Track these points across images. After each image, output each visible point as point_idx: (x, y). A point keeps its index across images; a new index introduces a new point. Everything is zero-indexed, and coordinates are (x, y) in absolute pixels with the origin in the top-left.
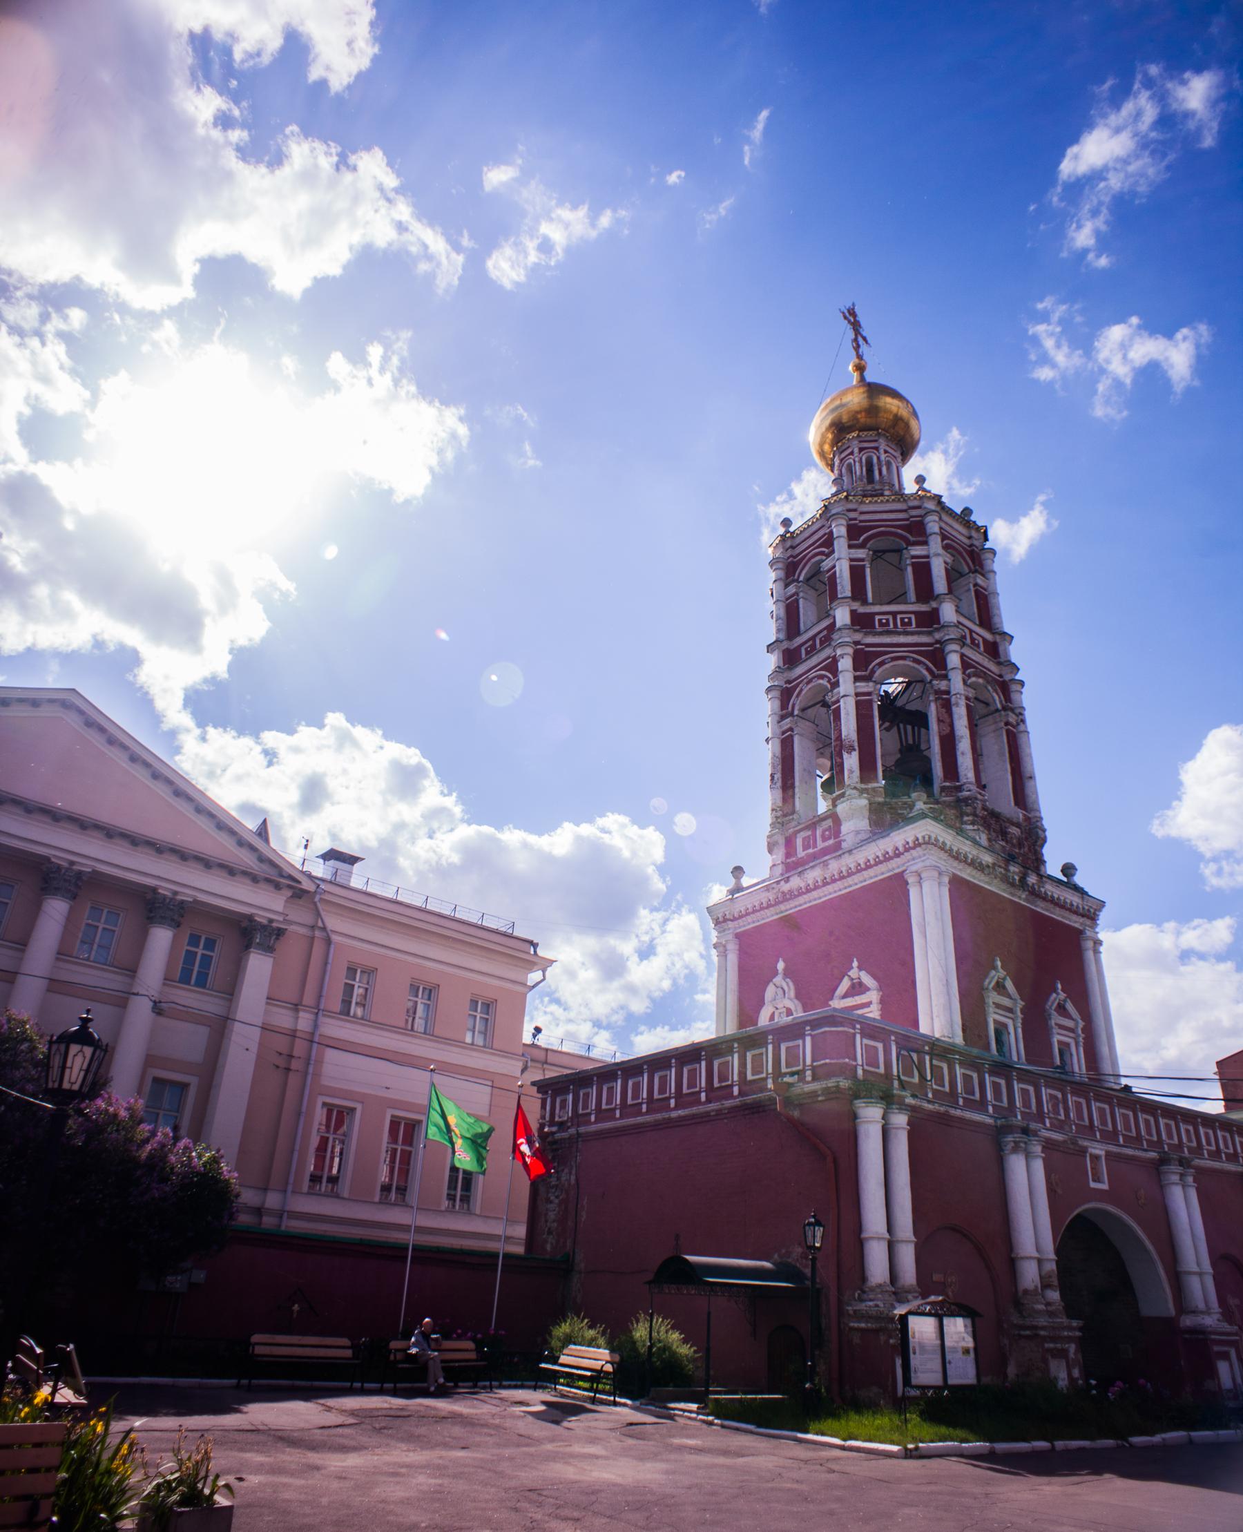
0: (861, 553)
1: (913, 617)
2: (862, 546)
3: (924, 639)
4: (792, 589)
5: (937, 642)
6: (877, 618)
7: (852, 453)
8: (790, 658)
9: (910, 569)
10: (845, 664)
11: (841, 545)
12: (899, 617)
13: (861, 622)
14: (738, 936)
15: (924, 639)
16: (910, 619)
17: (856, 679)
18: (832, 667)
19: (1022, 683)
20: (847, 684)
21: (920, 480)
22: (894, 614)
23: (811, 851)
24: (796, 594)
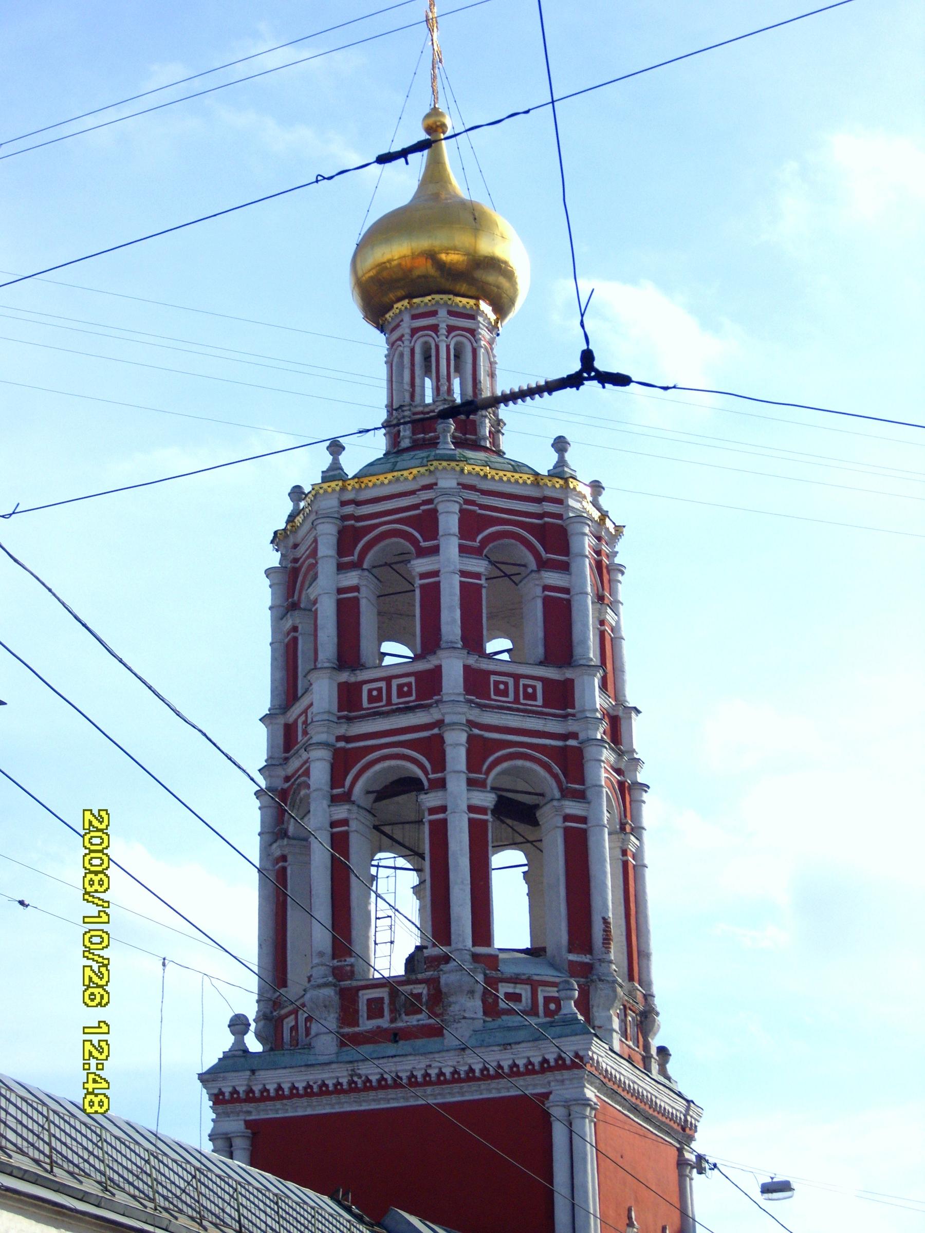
0: (478, 565)
1: (539, 686)
2: (477, 552)
3: (553, 726)
4: (351, 578)
5: (574, 735)
6: (493, 678)
7: (435, 328)
8: (348, 698)
9: (539, 604)
10: (457, 756)
11: (450, 547)
12: (522, 682)
13: (477, 683)
14: (248, 1124)
15: (553, 726)
16: (534, 688)
17: (471, 783)
18: (433, 748)
19: (644, 787)
20: (457, 784)
21: (560, 445)
22: (517, 677)
23: (384, 1023)
24: (356, 589)
